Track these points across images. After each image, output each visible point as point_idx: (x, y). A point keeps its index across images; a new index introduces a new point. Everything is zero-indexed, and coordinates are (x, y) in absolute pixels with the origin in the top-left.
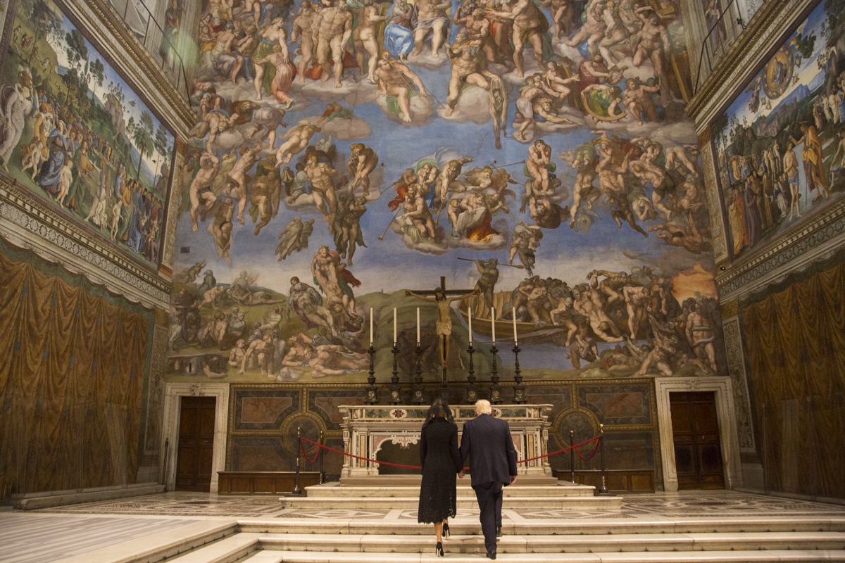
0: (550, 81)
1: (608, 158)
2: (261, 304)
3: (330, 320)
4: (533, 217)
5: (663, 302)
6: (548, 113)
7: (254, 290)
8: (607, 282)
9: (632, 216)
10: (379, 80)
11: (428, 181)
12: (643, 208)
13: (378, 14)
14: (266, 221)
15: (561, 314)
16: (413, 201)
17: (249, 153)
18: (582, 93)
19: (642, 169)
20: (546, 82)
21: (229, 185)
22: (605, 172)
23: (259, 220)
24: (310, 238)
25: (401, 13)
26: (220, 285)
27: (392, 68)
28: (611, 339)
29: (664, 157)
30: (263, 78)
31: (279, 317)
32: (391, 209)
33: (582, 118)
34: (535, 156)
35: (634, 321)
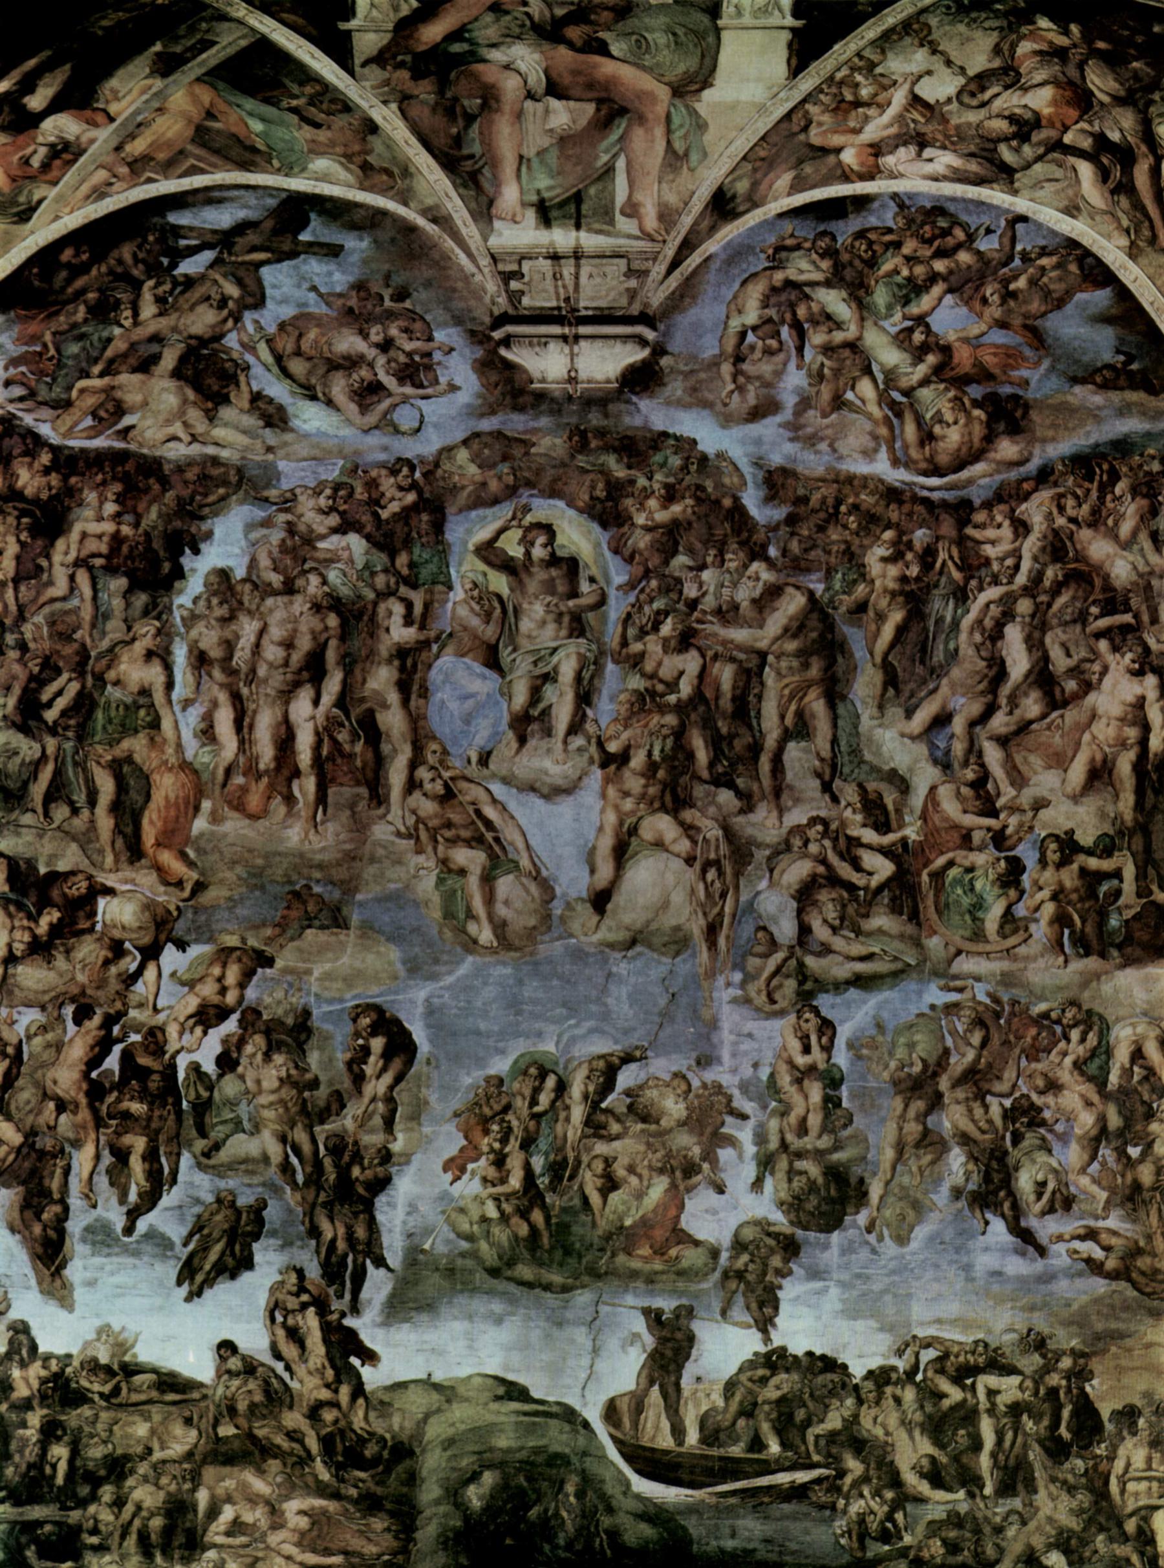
0: (849, 839)
1: (971, 1055)
2: (150, 1402)
3: (313, 1444)
4: (782, 1204)
5: (1066, 1413)
6: (835, 930)
7: (130, 1370)
8: (940, 1364)
9: (1015, 1206)
10: (416, 829)
11: (537, 1109)
12: (1043, 1184)
13: (408, 621)
14: (150, 1199)
15: (832, 1436)
16: (500, 1161)
17: (97, 1020)
18: (925, 877)
19: (1053, 1086)
20: (835, 840)
21: (51, 1105)
22: (960, 1094)
23: (133, 1197)
24: (256, 1246)
25: (475, 622)
26: (47, 1358)
27: (448, 796)
28: (940, 1495)
29: (1109, 1053)
30: (116, 807)
31: (194, 1433)
32: (449, 1176)
33: (918, 944)
34: (795, 1045)
35: (994, 1455)
